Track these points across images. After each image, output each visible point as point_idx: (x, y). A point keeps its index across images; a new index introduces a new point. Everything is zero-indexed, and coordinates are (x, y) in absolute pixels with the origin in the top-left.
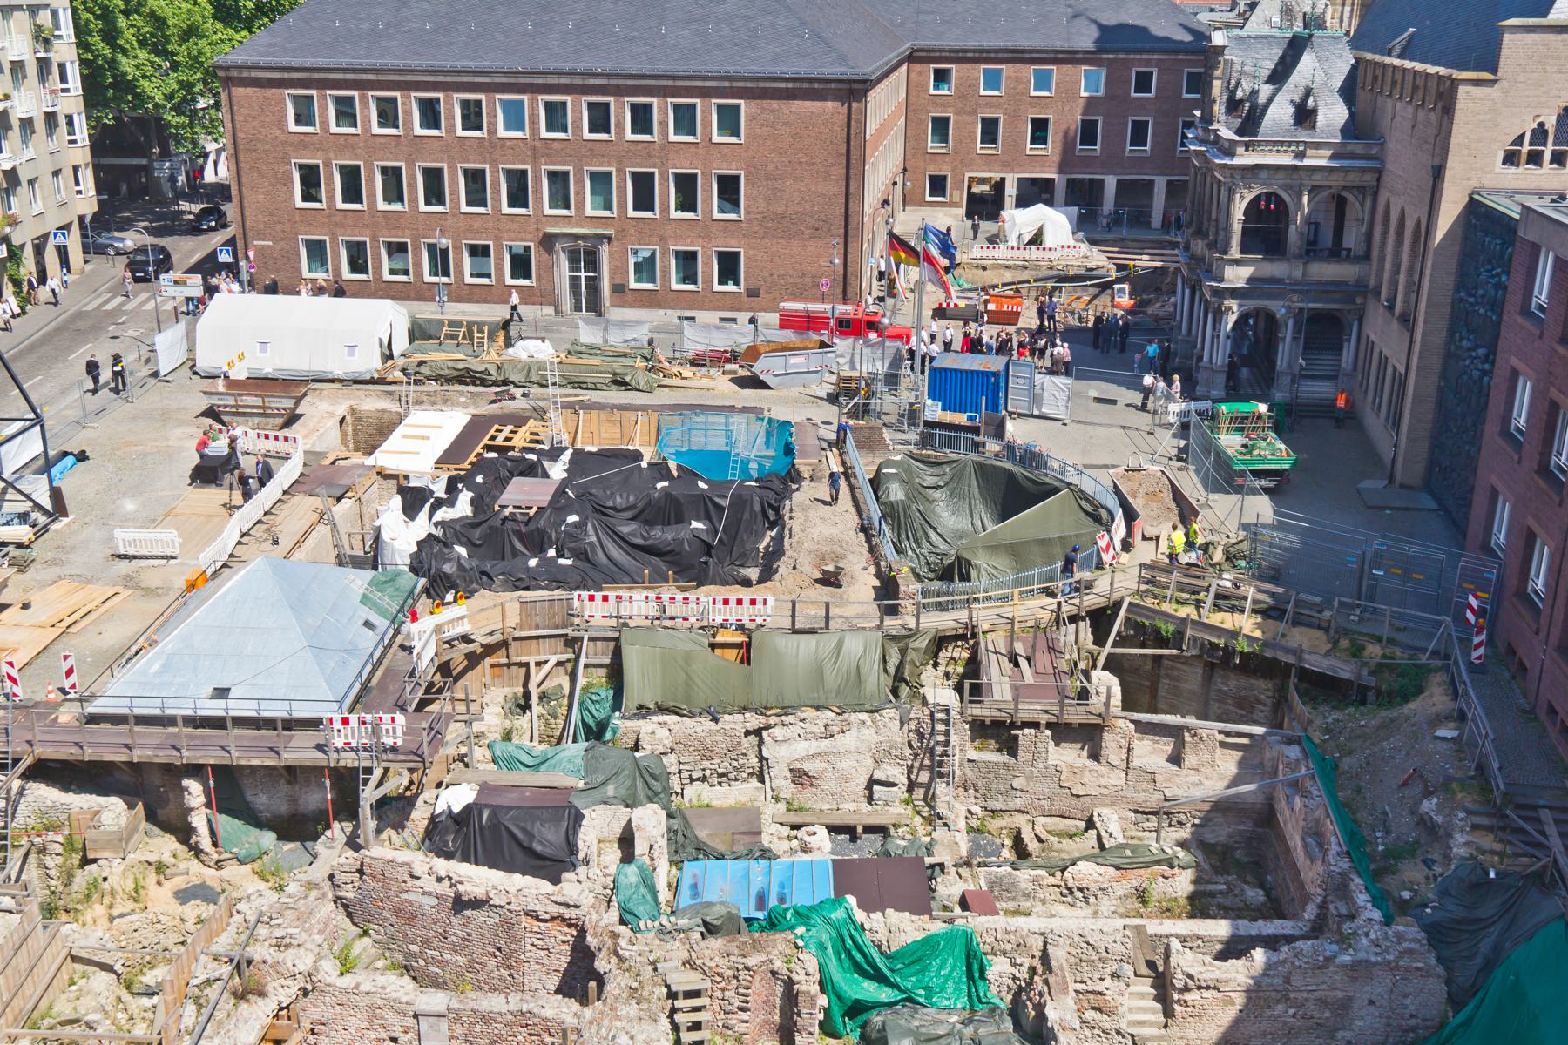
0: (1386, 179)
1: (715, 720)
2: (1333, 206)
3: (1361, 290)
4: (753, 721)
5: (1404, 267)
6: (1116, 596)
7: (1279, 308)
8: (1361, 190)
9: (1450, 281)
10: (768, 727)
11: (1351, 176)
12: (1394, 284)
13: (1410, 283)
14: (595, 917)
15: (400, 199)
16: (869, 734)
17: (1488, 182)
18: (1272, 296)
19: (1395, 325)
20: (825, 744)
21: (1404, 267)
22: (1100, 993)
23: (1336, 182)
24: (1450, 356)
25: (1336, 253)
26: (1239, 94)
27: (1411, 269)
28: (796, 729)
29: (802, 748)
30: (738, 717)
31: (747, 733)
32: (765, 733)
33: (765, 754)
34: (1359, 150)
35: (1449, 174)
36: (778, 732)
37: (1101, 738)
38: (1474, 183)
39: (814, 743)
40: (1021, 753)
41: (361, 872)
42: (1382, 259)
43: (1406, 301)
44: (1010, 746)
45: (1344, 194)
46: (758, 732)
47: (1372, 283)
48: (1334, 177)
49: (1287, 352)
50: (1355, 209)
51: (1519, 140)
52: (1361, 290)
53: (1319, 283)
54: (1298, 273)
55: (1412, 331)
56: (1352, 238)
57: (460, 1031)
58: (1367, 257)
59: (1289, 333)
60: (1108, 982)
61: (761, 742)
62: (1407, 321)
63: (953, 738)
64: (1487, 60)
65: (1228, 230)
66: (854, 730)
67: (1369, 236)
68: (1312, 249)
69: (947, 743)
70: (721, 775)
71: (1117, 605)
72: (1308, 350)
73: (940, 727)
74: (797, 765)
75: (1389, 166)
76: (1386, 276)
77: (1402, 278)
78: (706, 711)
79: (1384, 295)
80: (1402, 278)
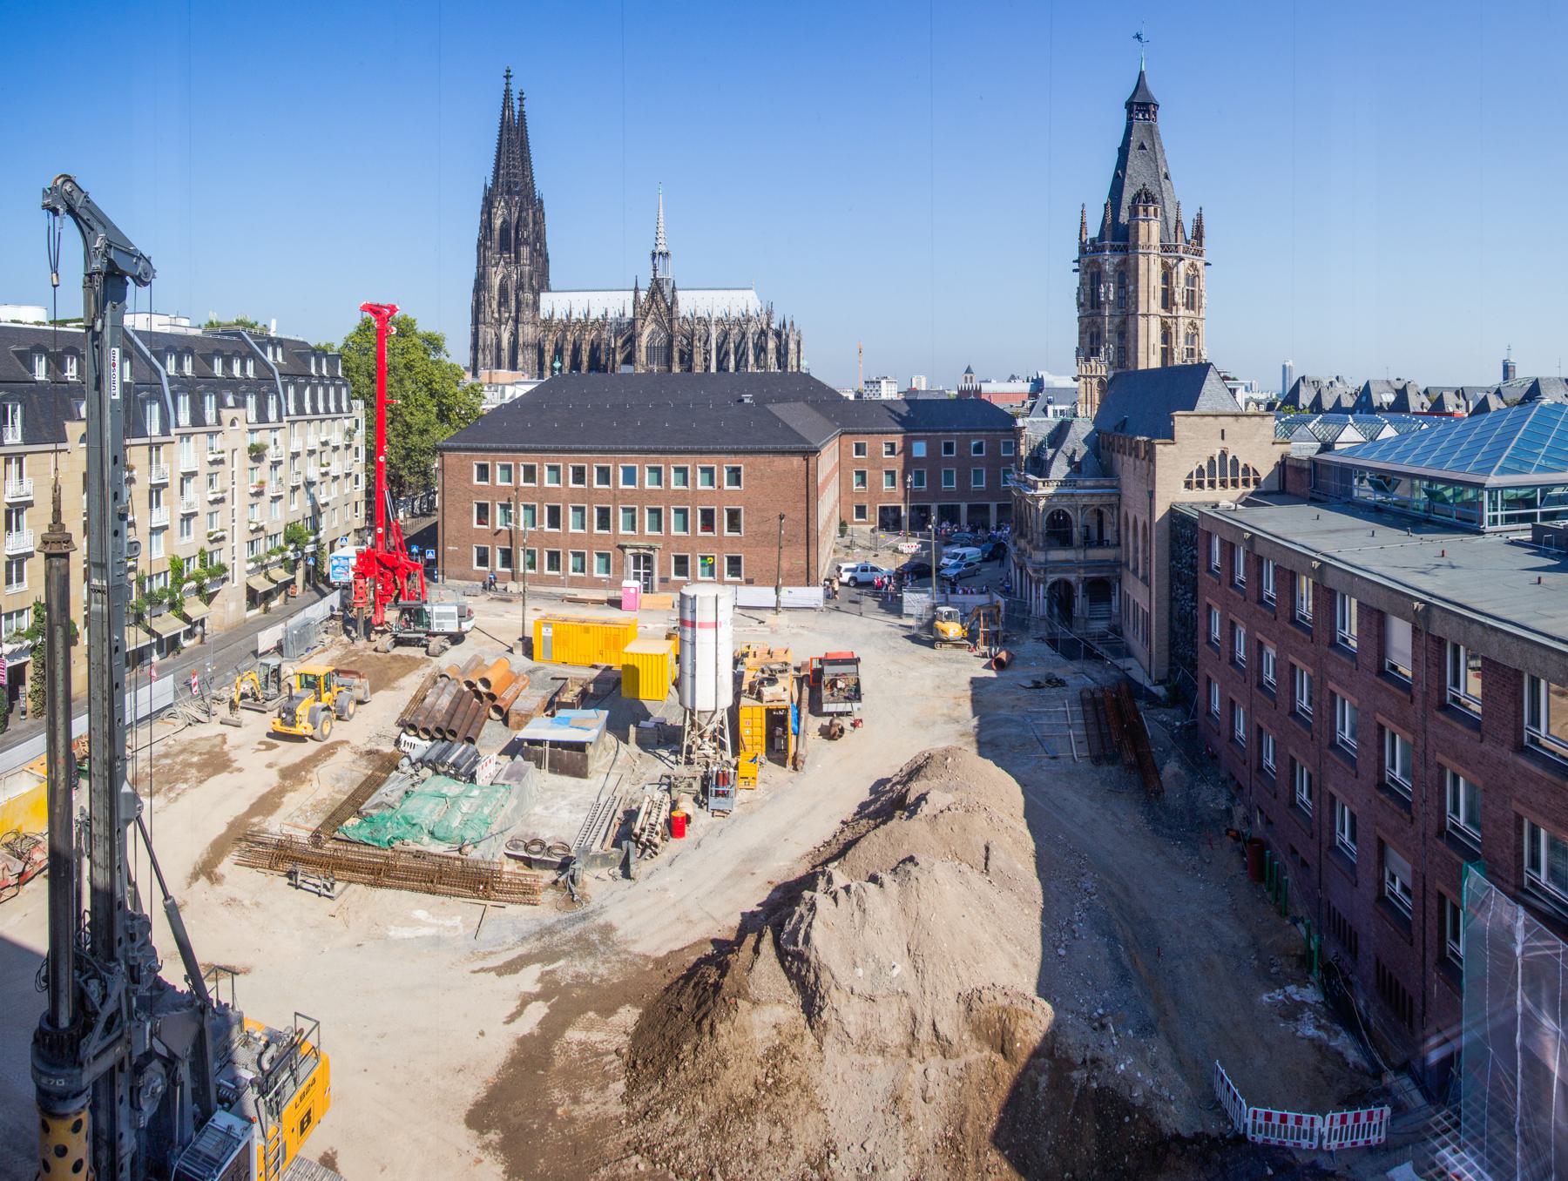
0: (1124, 499)
2: (1095, 516)
3: (1118, 564)
5: (1140, 550)
7: (1072, 577)
8: (1111, 505)
9: (1166, 557)
11: (1104, 498)
13: (1144, 559)
17: (1178, 499)
18: (1067, 571)
19: (1140, 584)
21: (1140, 550)
23: (1096, 501)
25: (1101, 543)
27: (1144, 551)
34: (1107, 484)
35: (1157, 495)
38: (1171, 500)
42: (1127, 545)
43: (1144, 569)
47: (1123, 560)
48: (1095, 499)
49: (1080, 603)
50: (1108, 517)
51: (1191, 475)
52: (1118, 564)
53: (1094, 561)
54: (1081, 557)
56: (1109, 534)
58: (1119, 544)
59: (1080, 592)
64: (1169, 435)
67: (1118, 531)
72: (1093, 601)
75: (1124, 492)
76: (1131, 554)
77: (1140, 556)
80: (1140, 556)
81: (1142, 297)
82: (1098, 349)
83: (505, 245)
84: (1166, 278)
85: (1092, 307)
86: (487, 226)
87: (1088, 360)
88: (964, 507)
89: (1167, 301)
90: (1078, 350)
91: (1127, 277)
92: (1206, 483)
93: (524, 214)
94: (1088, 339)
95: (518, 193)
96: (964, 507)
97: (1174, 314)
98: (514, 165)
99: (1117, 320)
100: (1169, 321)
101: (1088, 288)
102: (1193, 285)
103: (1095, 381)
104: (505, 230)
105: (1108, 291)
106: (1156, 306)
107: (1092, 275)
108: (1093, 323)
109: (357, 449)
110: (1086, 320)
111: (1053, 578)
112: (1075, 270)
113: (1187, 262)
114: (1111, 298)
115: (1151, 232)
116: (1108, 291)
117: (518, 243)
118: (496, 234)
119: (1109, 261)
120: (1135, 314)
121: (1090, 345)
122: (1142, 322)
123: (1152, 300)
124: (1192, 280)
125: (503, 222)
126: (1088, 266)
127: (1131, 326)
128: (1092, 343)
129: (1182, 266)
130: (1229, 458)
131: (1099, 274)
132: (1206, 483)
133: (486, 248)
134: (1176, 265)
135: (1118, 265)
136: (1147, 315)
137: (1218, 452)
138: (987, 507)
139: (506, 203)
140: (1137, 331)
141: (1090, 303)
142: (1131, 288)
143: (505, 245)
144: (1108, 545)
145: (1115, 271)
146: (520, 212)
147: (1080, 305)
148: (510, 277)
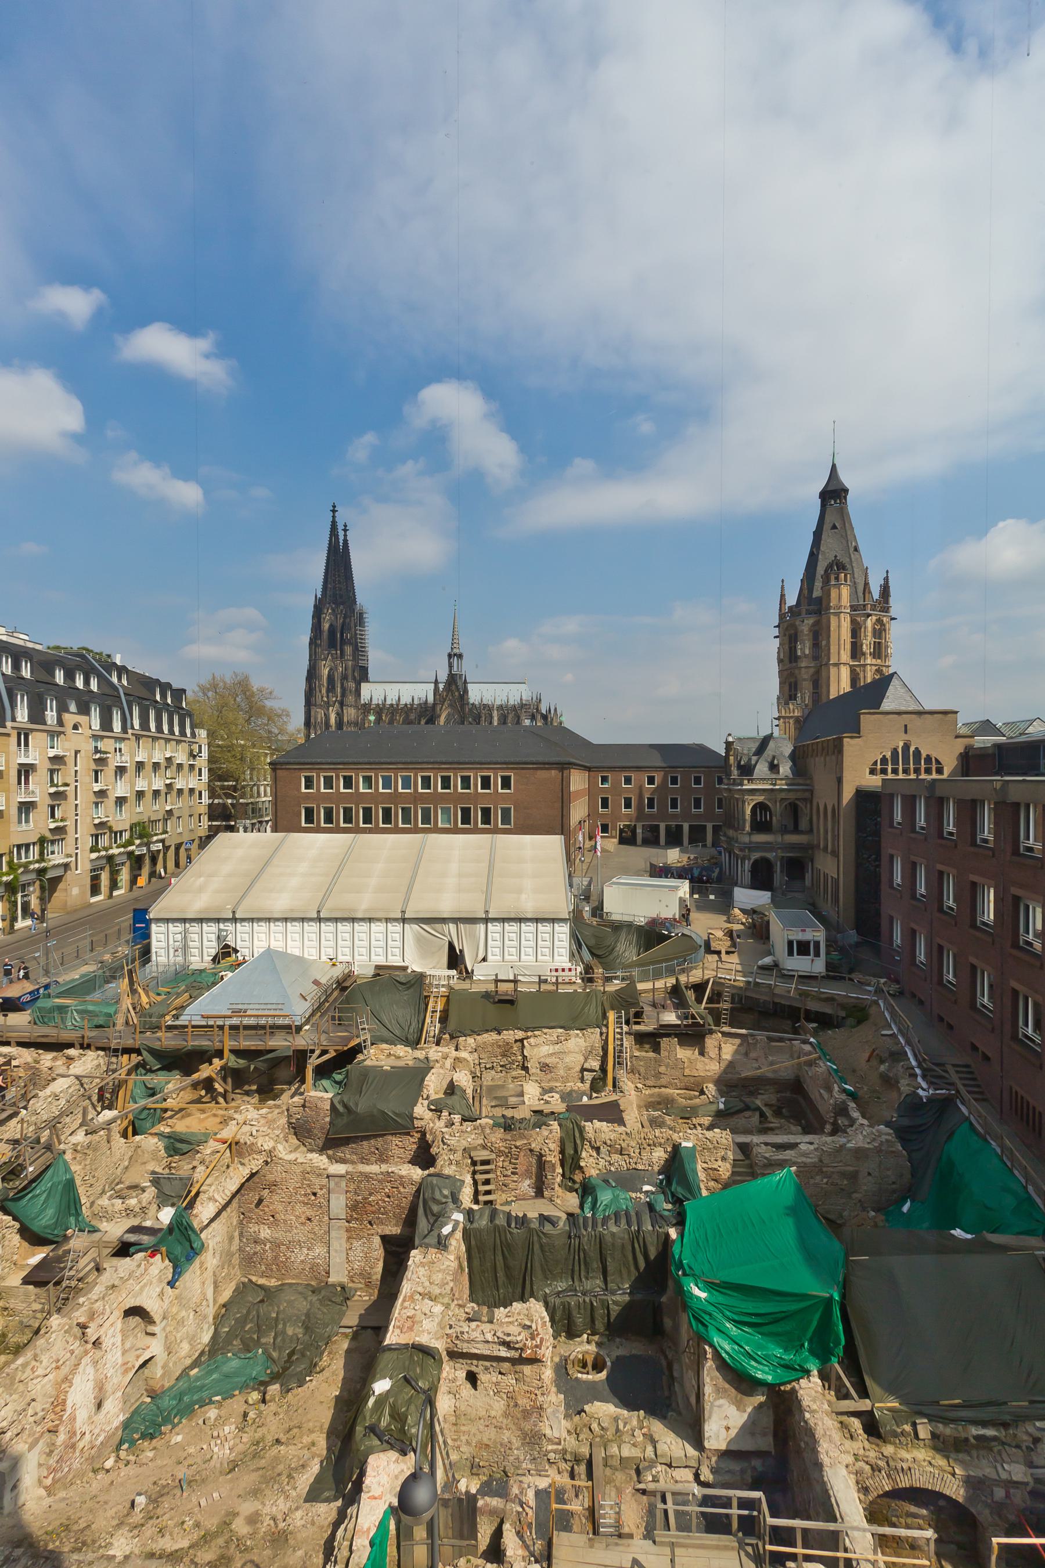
1: (499, 1033)
4: (520, 1034)
6: (706, 977)
7: (770, 856)
10: (527, 1038)
12: (826, 839)
14: (431, 1125)
15: (350, 822)
16: (581, 1042)
20: (557, 1047)
22: (716, 1169)
24: (858, 865)
26: (742, 763)
28: (540, 1040)
29: (545, 1050)
30: (511, 1032)
31: (516, 1041)
32: (525, 1042)
33: (526, 1053)
36: (532, 1040)
37: (704, 1042)
39: (552, 1047)
40: (662, 1052)
41: (304, 1106)
44: (656, 1049)
45: (798, 802)
46: (522, 1041)
54: (779, 839)
55: (838, 857)
56: (803, 824)
57: (352, 1187)
60: (720, 1163)
61: (523, 1046)
62: (835, 854)
63: (626, 1044)
65: (744, 820)
66: (573, 1039)
68: (784, 831)
69: (622, 1045)
70: (502, 1066)
71: (708, 981)
73: (619, 1036)
74: (542, 1060)
78: (495, 1029)
79: (822, 846)
81: (833, 649)
82: (796, 695)
83: (332, 644)
84: (855, 632)
85: (791, 662)
86: (317, 627)
87: (787, 704)
88: (686, 827)
89: (856, 651)
90: (778, 698)
91: (820, 635)
92: (890, 770)
93: (348, 620)
94: (787, 688)
95: (343, 603)
96: (686, 827)
97: (862, 662)
98: (340, 582)
99: (812, 670)
100: (858, 669)
101: (787, 647)
102: (880, 638)
103: (791, 721)
104: (332, 630)
105: (804, 648)
106: (845, 656)
107: (790, 637)
108: (792, 674)
109: (200, 770)
110: (786, 673)
111: (756, 856)
112: (776, 637)
113: (874, 618)
114: (807, 652)
115: (843, 595)
116: (804, 648)
117: (343, 642)
118: (325, 635)
119: (806, 626)
120: (827, 664)
121: (789, 689)
122: (833, 671)
123: (842, 652)
124: (880, 631)
125: (331, 625)
126: (787, 629)
127: (824, 674)
128: (790, 690)
129: (870, 623)
130: (912, 749)
131: (796, 635)
132: (890, 770)
133: (316, 645)
134: (865, 621)
135: (814, 625)
136: (837, 665)
137: (901, 744)
138: (705, 826)
139: (333, 610)
140: (829, 677)
141: (788, 658)
142: (824, 643)
143: (332, 644)
144: (802, 832)
145: (810, 630)
146: (345, 618)
147: (780, 661)
148: (337, 669)
